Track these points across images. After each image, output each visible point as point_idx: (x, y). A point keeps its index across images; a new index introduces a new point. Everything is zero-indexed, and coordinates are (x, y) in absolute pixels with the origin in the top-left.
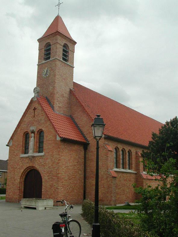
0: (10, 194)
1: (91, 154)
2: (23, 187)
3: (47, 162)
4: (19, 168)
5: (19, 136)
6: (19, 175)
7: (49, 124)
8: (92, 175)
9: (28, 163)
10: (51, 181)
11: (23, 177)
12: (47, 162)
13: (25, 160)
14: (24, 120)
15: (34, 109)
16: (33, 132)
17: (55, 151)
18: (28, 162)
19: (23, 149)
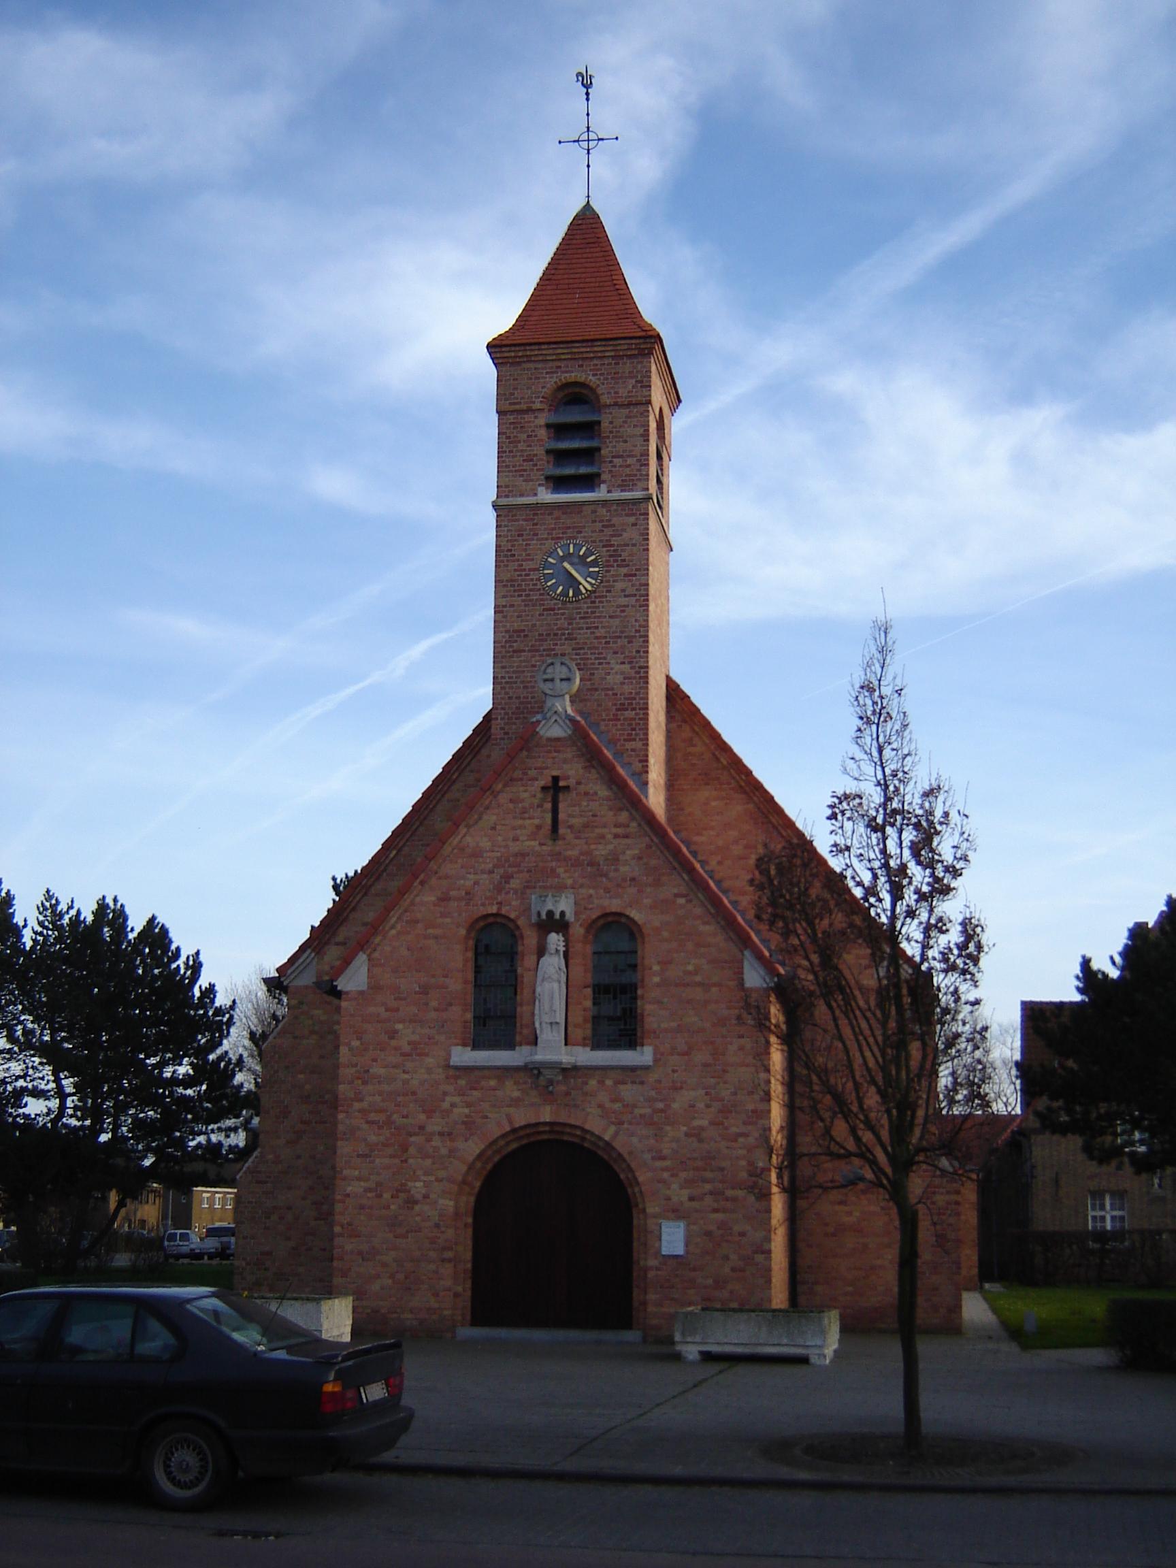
0: (376, 1287)
2: (470, 1243)
4: (441, 1134)
5: (426, 937)
7: (675, 891)
9: (516, 1102)
10: (716, 1211)
13: (493, 1083)
14: (469, 839)
15: (544, 789)
18: (516, 1102)
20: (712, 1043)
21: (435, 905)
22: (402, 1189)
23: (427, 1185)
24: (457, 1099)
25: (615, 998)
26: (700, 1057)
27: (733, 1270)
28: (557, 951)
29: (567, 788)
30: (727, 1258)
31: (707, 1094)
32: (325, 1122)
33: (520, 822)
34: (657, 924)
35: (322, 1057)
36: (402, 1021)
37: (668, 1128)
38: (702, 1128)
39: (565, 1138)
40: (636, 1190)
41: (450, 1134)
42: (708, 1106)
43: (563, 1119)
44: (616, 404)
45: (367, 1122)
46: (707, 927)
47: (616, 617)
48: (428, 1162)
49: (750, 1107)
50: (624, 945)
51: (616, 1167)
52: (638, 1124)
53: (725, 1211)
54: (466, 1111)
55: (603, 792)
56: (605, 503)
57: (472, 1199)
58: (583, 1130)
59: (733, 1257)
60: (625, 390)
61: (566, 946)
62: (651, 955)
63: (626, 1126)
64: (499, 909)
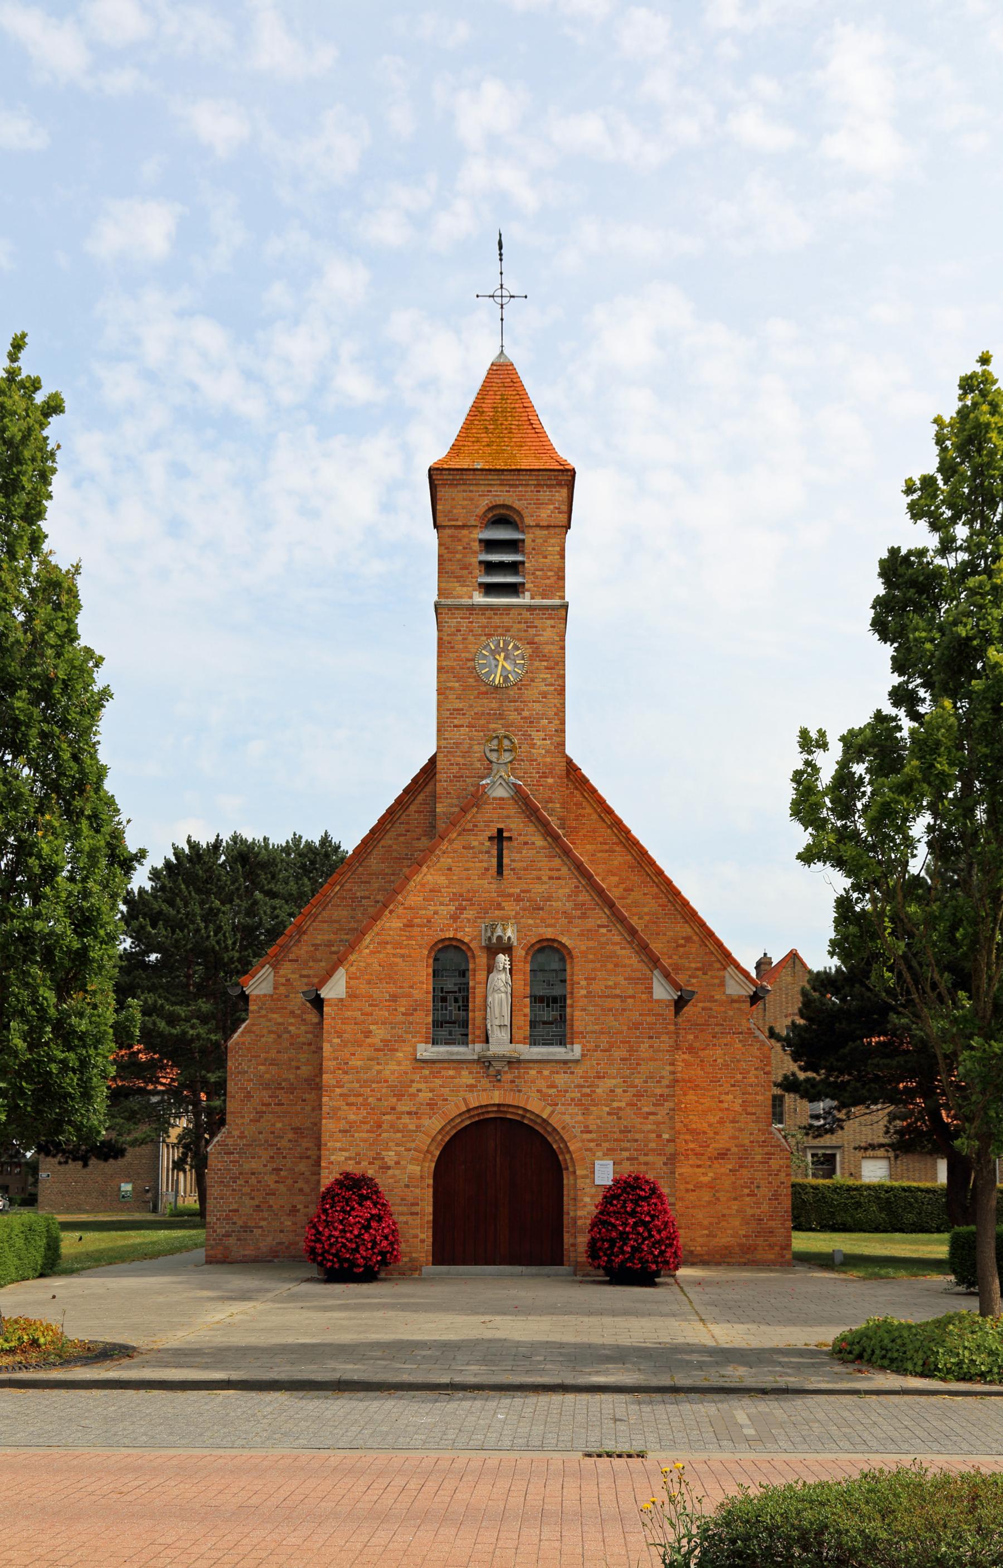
1: (685, 1056)
3: (598, 1090)
4: (409, 1113)
8: (692, 1146)
12: (598, 1090)
13: (451, 1073)
14: (429, 877)
15: (490, 839)
16: (497, 947)
18: (471, 1088)
20: (629, 1042)
21: (401, 930)
22: (378, 1157)
23: (398, 1154)
24: (423, 1086)
26: (618, 1054)
28: (504, 968)
29: (510, 838)
32: (283, 1104)
33: (472, 865)
34: (583, 948)
35: (279, 1052)
36: (377, 1023)
37: (594, 1108)
38: (619, 1108)
39: (509, 1116)
40: (568, 1157)
41: (416, 1113)
42: (624, 1091)
43: (509, 1101)
44: (537, 526)
45: (347, 1104)
46: (623, 952)
48: (399, 1135)
49: (658, 1091)
50: (555, 966)
51: (549, 1139)
52: (570, 1105)
54: (430, 1095)
55: (540, 842)
56: (530, 608)
57: (433, 1165)
58: (526, 1110)
60: (545, 514)
61: (511, 965)
62: (578, 973)
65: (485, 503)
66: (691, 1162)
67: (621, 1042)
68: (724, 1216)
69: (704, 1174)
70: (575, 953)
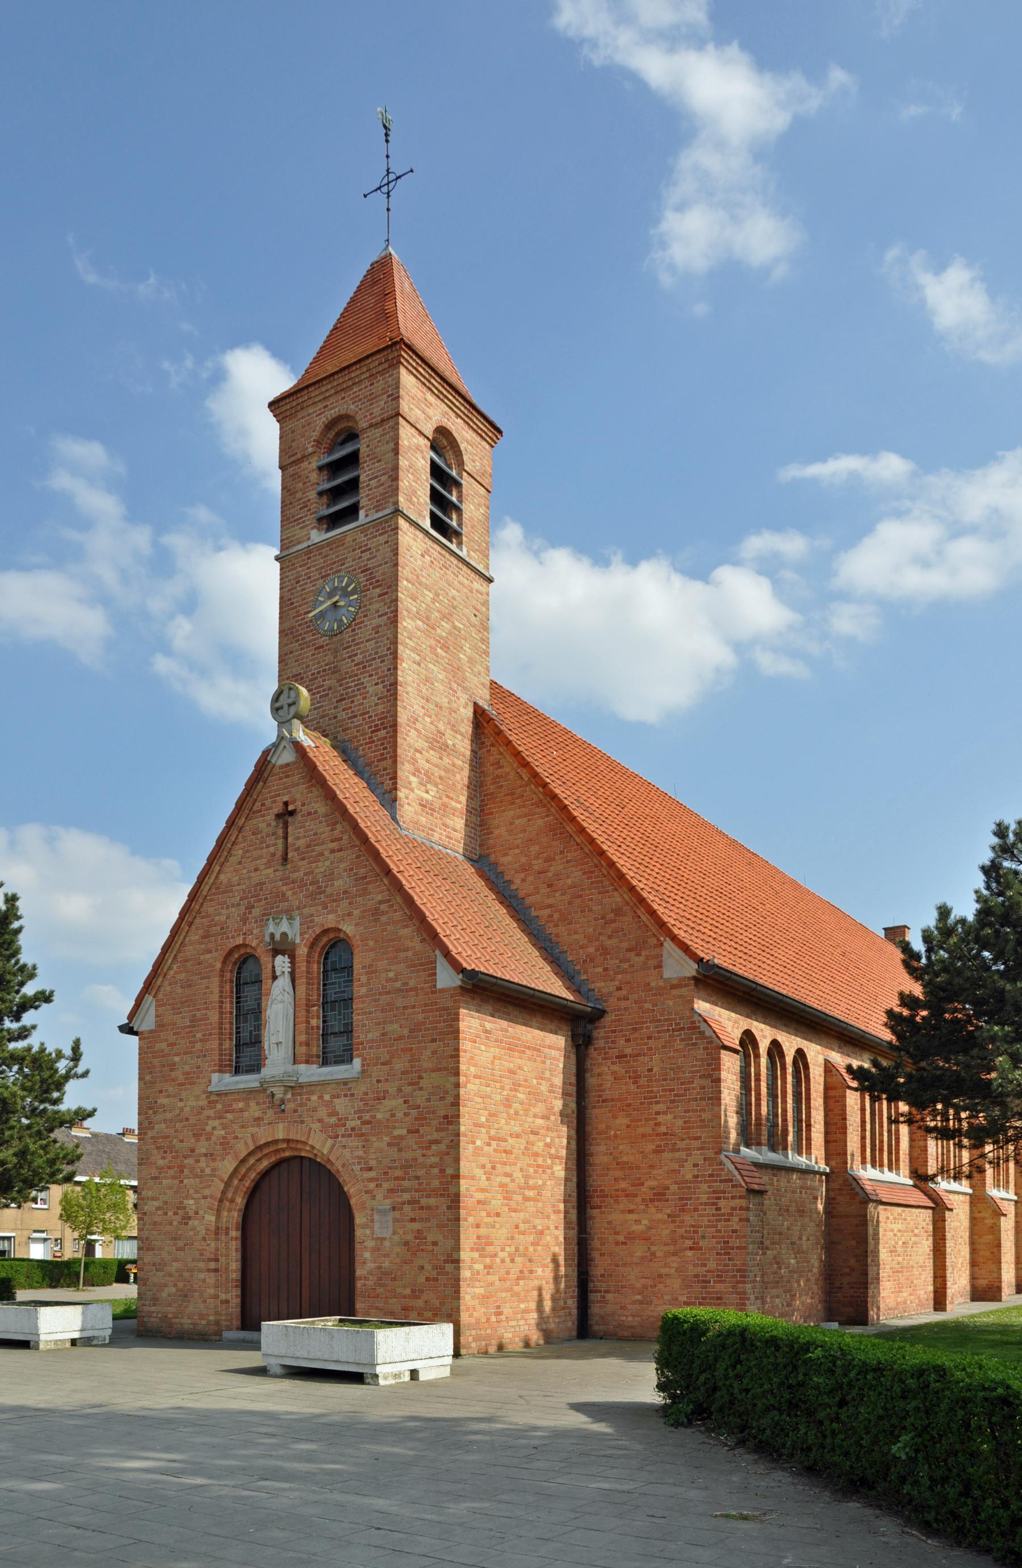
1: (614, 1068)
4: (205, 1155)
6: (207, 1192)
7: (379, 898)
8: (623, 1185)
10: (413, 1220)
11: (232, 1201)
13: (241, 1105)
14: (222, 877)
15: (278, 816)
16: (281, 947)
17: (428, 1053)
19: (227, 1045)
20: (411, 1049)
22: (181, 1207)
25: (340, 1014)
27: (427, 1279)
30: (422, 1268)
31: (405, 1102)
37: (374, 1139)
38: (401, 1137)
47: (371, 639)
49: (442, 1113)
52: (350, 1136)
53: (421, 1220)
54: (223, 1132)
59: (428, 1267)
63: (340, 1139)
64: (244, 939)
65: (320, 422)
66: (621, 1207)
67: (403, 1050)
68: (660, 1276)
69: (638, 1222)
70: (356, 942)
